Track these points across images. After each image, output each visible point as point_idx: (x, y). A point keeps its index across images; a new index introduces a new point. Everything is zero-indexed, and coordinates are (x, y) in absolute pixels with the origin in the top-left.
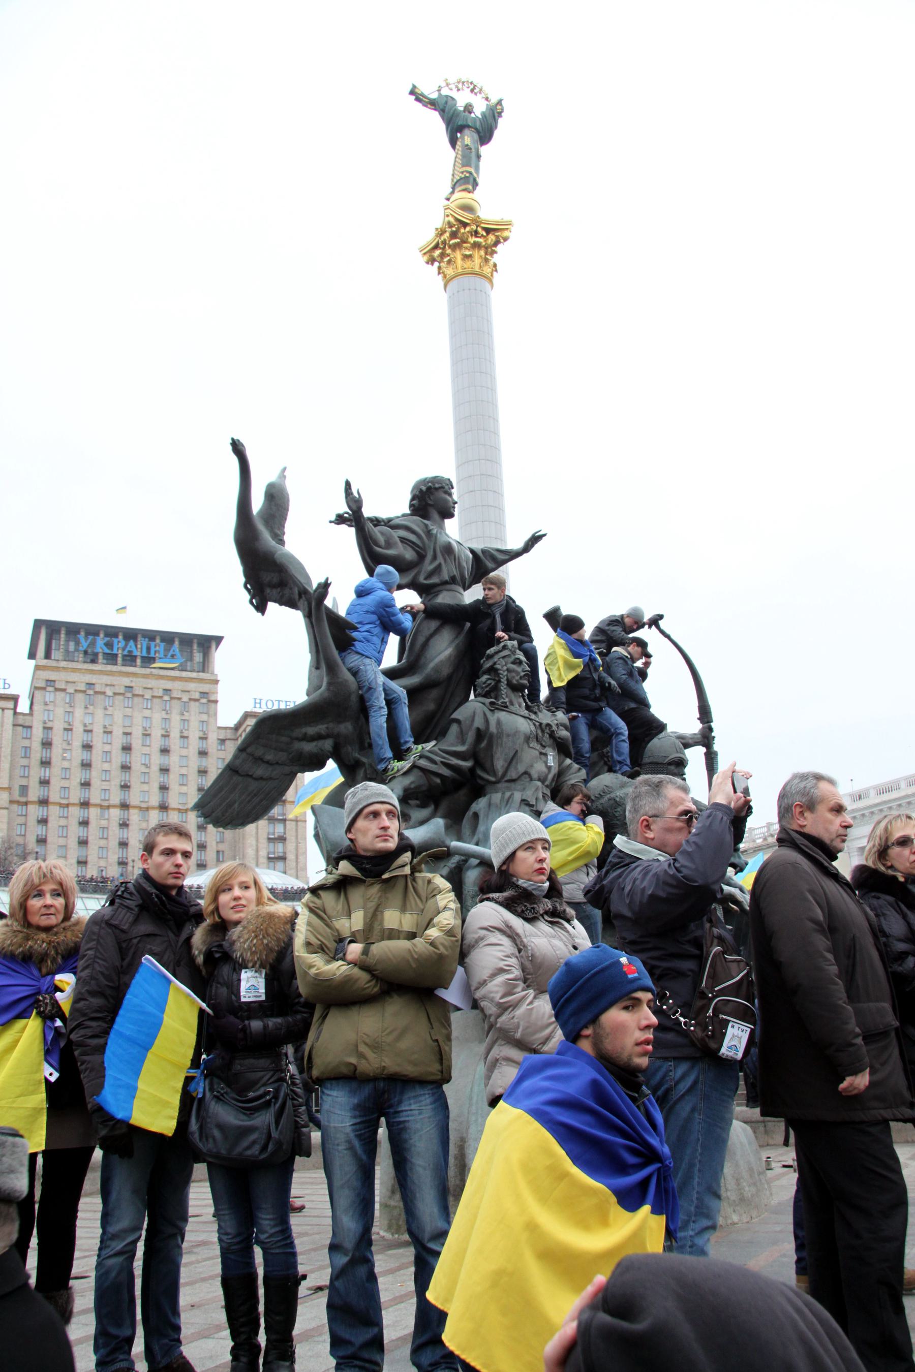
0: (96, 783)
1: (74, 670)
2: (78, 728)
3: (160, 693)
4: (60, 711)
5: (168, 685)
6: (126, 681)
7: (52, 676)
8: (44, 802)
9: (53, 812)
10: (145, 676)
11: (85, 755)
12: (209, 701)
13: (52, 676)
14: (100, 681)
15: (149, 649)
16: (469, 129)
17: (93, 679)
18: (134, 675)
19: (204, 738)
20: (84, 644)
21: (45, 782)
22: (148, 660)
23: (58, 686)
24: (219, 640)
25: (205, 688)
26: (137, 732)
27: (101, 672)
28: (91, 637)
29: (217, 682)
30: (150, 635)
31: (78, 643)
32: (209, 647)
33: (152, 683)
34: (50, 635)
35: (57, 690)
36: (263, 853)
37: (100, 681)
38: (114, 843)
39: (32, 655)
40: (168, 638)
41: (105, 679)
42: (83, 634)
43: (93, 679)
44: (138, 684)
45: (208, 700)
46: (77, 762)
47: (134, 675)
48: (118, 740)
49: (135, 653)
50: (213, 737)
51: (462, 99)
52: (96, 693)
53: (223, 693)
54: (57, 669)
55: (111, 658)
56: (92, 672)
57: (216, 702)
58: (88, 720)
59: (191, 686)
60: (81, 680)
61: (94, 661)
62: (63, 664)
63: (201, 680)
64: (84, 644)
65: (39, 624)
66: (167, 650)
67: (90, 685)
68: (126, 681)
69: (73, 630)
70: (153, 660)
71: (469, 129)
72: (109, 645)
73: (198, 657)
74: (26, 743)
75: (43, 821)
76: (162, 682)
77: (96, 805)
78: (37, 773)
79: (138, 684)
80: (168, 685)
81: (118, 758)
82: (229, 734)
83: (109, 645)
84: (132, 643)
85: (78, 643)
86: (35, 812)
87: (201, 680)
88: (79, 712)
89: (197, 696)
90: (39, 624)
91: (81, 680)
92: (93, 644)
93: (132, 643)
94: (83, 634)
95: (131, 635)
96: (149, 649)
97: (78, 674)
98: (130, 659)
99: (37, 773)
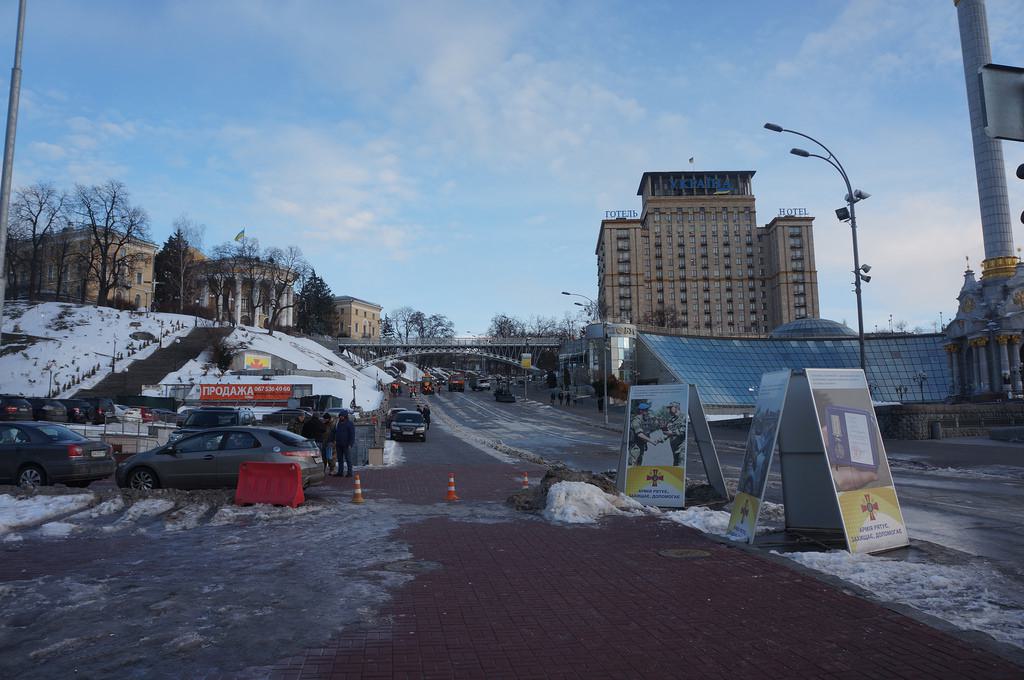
0: (688, 266)
1: (670, 201)
2: (675, 235)
3: (720, 210)
4: (664, 226)
5: (725, 204)
6: (700, 204)
8: (660, 280)
9: (667, 285)
10: (711, 200)
11: (680, 251)
12: (750, 212)
14: (685, 206)
15: (711, 184)
17: (679, 205)
18: (704, 200)
19: (749, 235)
20: (673, 185)
21: (659, 268)
22: (712, 191)
24: (753, 173)
25: (747, 204)
26: (709, 235)
27: (688, 201)
28: (676, 180)
29: (754, 200)
30: (711, 175)
31: (669, 184)
32: (747, 178)
33: (715, 204)
35: (660, 213)
36: (792, 304)
37: (685, 206)
40: (722, 175)
41: (688, 205)
43: (679, 205)
44: (706, 205)
45: (750, 212)
46: (676, 256)
47: (704, 200)
48: (699, 240)
50: (754, 234)
52: (683, 213)
53: (758, 206)
54: (660, 201)
55: (690, 192)
56: (680, 200)
57: (755, 212)
58: (680, 230)
59: (739, 204)
60: (674, 206)
61: (680, 194)
62: (663, 198)
63: (745, 200)
64: (673, 185)
66: (722, 183)
67: (680, 209)
68: (700, 204)
69: (666, 176)
72: (688, 184)
75: (661, 291)
76: (722, 203)
77: (690, 280)
78: (654, 263)
79: (706, 205)
80: (725, 204)
82: (765, 232)
83: (688, 184)
84: (701, 181)
85: (669, 184)
86: (656, 285)
87: (745, 200)
88: (675, 226)
89: (742, 209)
91: (674, 206)
92: (679, 183)
93: (701, 181)
95: (700, 175)
96: (711, 184)
97: (673, 203)
98: (701, 191)
99: (654, 263)
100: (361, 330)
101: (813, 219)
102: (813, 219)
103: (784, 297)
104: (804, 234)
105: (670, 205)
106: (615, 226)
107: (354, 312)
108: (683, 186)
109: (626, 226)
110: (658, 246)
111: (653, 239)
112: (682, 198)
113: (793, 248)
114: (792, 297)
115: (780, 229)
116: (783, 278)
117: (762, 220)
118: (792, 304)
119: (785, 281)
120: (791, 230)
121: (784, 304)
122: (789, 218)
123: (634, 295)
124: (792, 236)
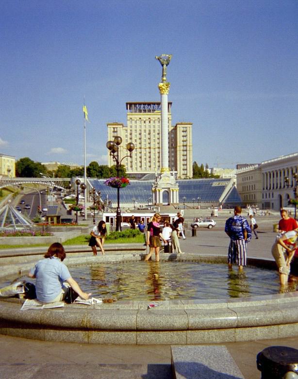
2: (138, 129)
3: (157, 119)
6: (149, 116)
10: (153, 115)
14: (142, 117)
22: (154, 110)
24: (171, 103)
27: (143, 115)
37: (142, 117)
38: (147, 157)
39: (127, 109)
43: (140, 117)
49: (151, 109)
54: (132, 115)
55: (145, 111)
56: (140, 115)
61: (141, 112)
65: (127, 104)
67: (140, 118)
68: (149, 116)
70: (155, 110)
72: (144, 107)
74: (126, 134)
81: (148, 136)
90: (127, 104)
92: (140, 107)
98: (149, 111)
100: (7, 168)
105: (136, 116)
107: (3, 161)
110: (131, 134)
111: (129, 132)
112: (141, 113)
113: (183, 136)
114: (181, 156)
115: (178, 129)
124: (183, 131)
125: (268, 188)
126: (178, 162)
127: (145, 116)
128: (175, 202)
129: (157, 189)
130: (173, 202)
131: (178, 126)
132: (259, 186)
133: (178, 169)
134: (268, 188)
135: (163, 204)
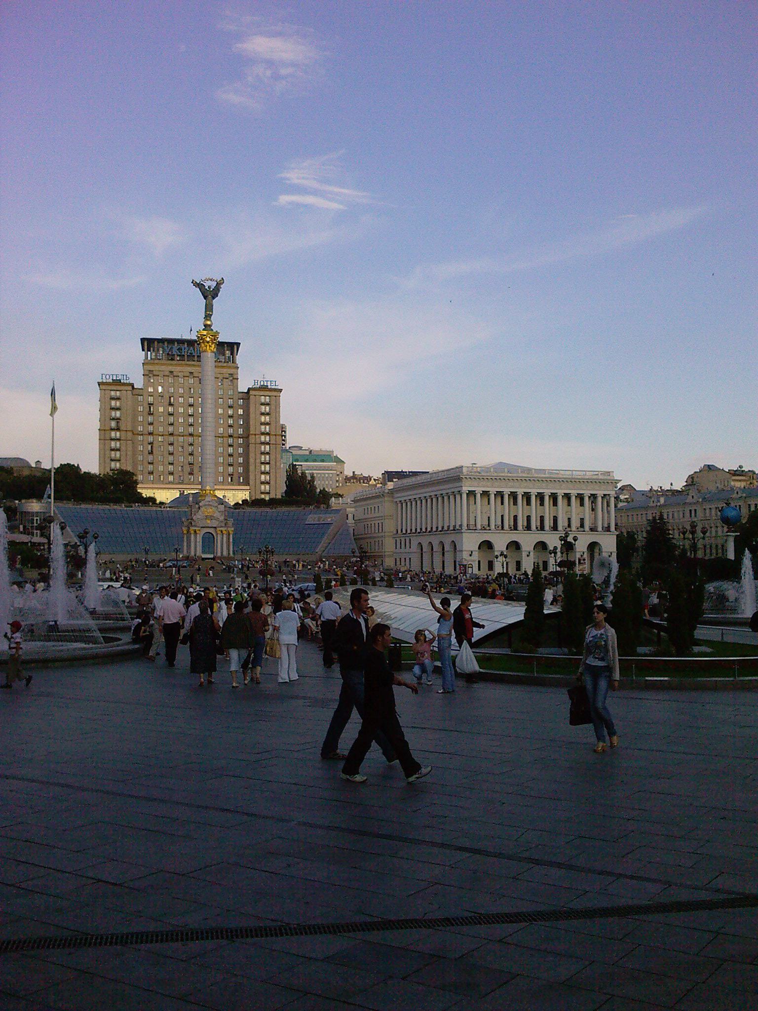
6: (190, 369)
7: (151, 368)
13: (151, 368)
16: (210, 294)
17: (171, 368)
23: (155, 373)
24: (238, 344)
34: (148, 344)
36: (258, 461)
37: (176, 369)
39: (143, 350)
41: (179, 368)
42: (166, 344)
43: (171, 368)
45: (234, 378)
51: (207, 284)
56: (171, 364)
59: (225, 370)
60: (167, 369)
61: (172, 359)
65: (143, 340)
71: (210, 294)
73: (228, 353)
87: (230, 367)
89: (227, 376)
90: (143, 340)
94: (166, 344)
98: (191, 357)
101: (281, 390)
102: (281, 390)
103: (252, 455)
104: (273, 403)
105: (163, 368)
106: (110, 387)
108: (175, 351)
109: (119, 388)
116: (252, 439)
117: (243, 387)
118: (258, 461)
119: (253, 441)
120: (263, 399)
121: (252, 460)
122: (264, 388)
123: (123, 448)
125: (404, 532)
126: (252, 468)
127: (180, 368)
128: (225, 553)
129: (192, 529)
130: (222, 553)
131: (251, 392)
132: (390, 526)
133: (251, 482)
134: (404, 532)
135: (204, 556)
